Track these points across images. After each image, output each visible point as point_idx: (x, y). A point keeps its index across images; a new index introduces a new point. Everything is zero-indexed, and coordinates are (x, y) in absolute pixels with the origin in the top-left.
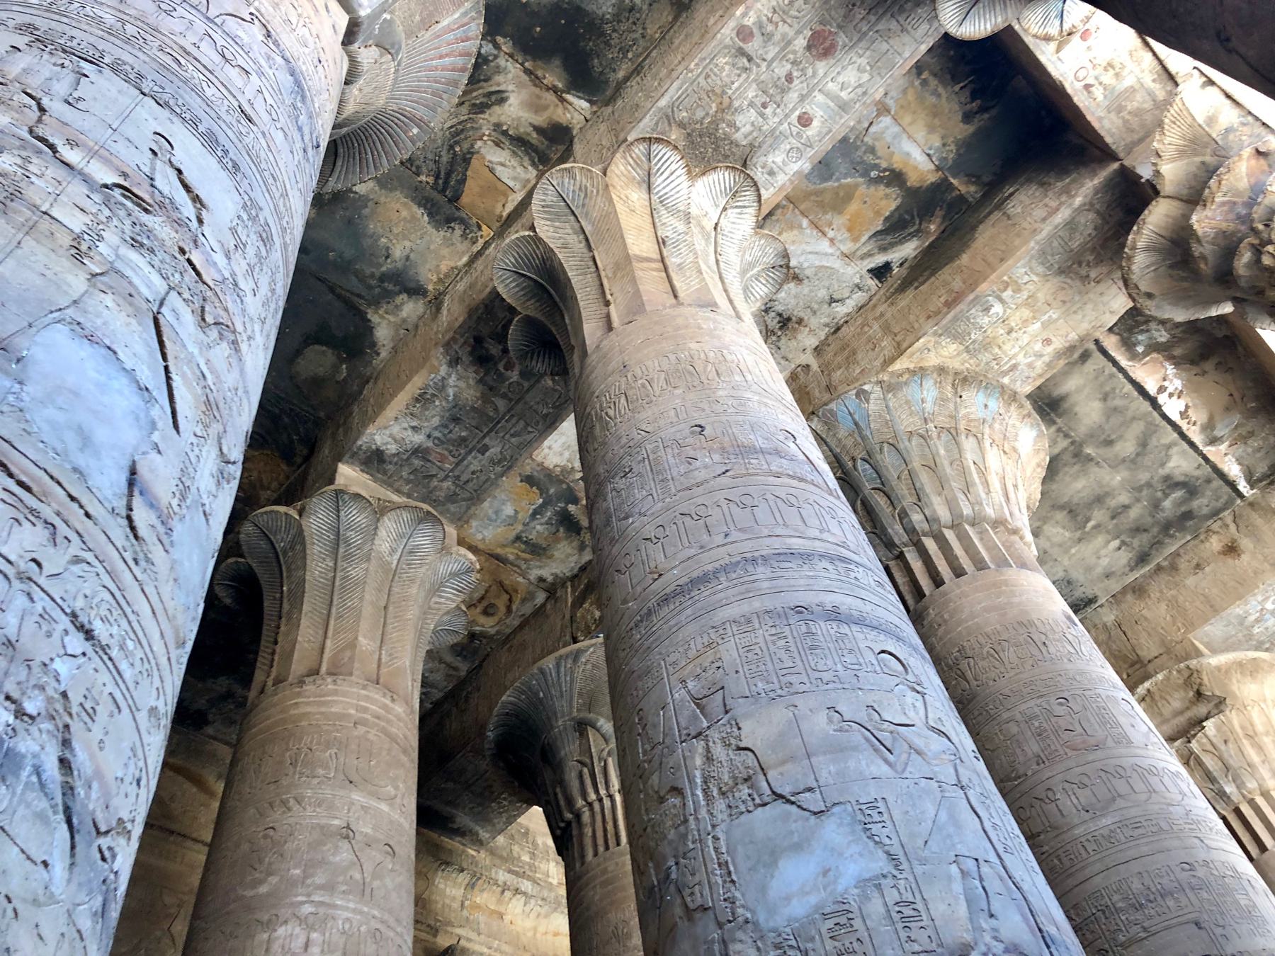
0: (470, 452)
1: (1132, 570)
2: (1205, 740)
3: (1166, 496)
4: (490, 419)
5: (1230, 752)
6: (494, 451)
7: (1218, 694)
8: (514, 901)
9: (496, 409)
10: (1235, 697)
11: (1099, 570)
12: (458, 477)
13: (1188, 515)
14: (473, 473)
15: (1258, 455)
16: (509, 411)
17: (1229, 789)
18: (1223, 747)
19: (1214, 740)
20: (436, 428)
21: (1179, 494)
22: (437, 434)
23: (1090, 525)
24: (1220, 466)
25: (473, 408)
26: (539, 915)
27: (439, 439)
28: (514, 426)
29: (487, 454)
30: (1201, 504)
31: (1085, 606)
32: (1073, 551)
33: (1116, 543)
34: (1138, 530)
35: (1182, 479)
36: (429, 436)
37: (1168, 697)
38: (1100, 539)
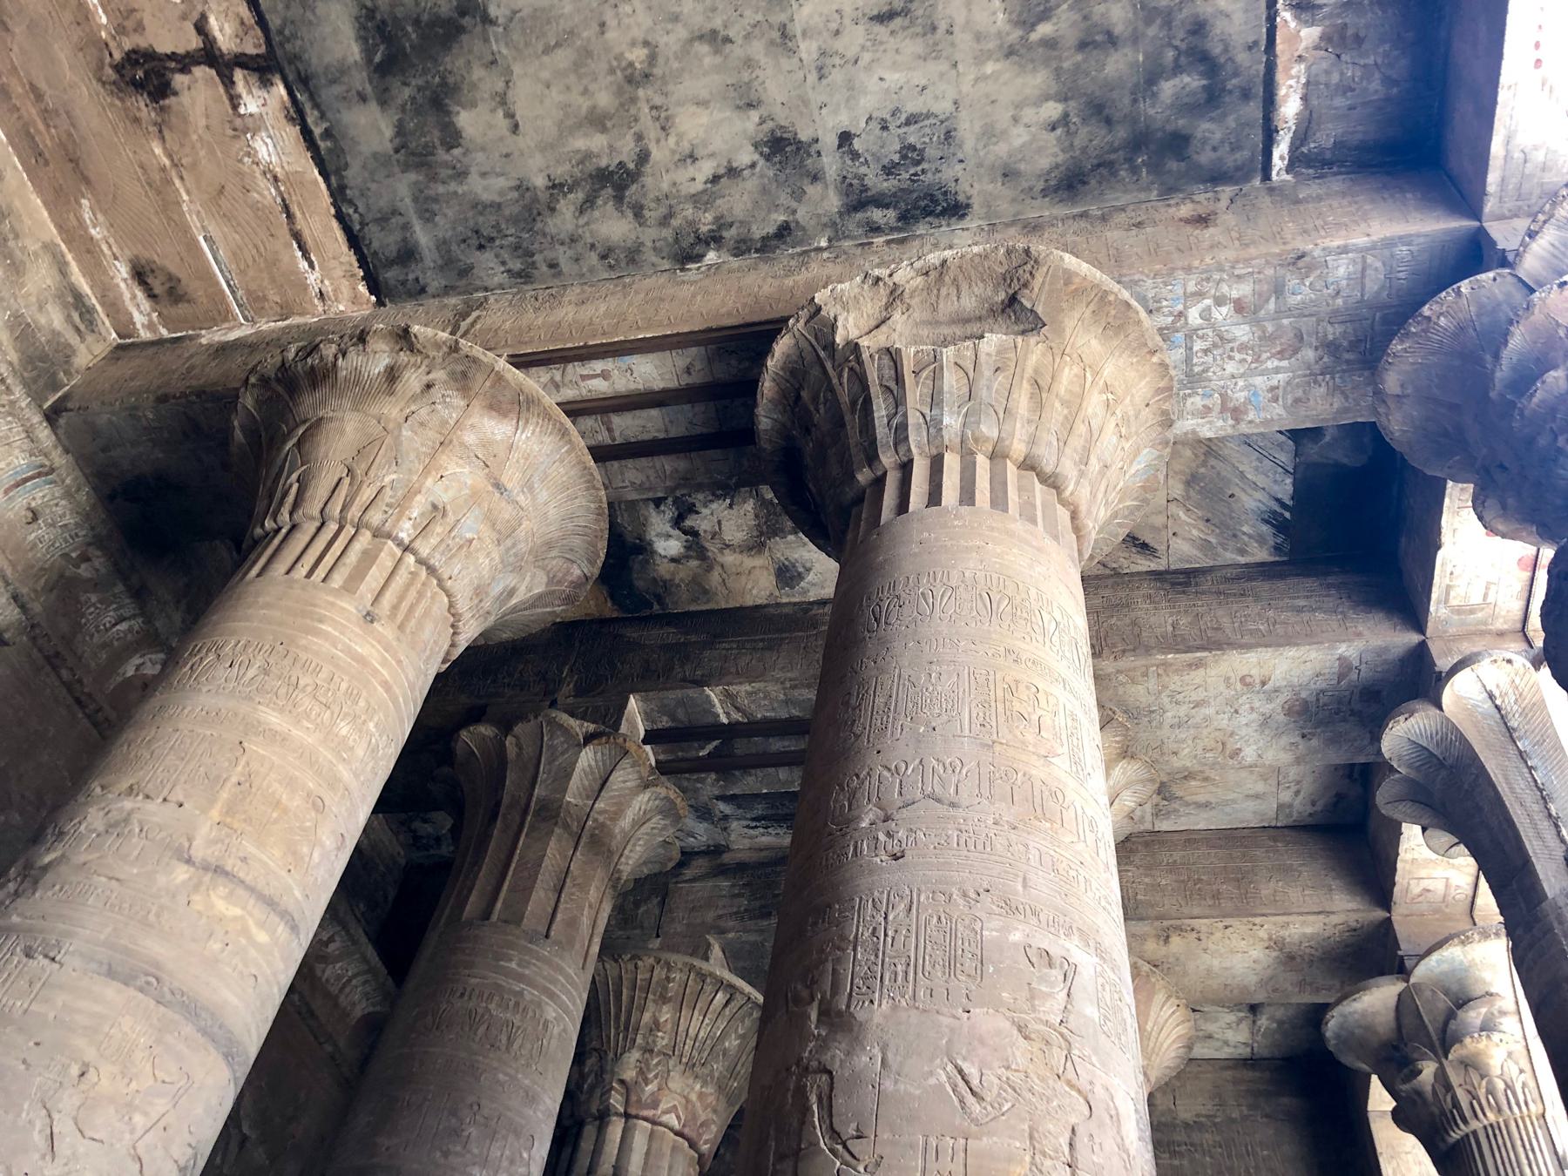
1: (1045, 193)
2: (969, 354)
3: (1177, 69)
5: (991, 387)
7: (1039, 310)
10: (1059, 331)
11: (1001, 149)
13: (1178, 143)
15: (1340, 102)
17: (951, 422)
18: (987, 373)
19: (982, 358)
21: (1192, 81)
23: (1044, 29)
24: (1280, 76)
30: (1208, 130)
31: (943, 213)
32: (990, 68)
33: (1053, 110)
34: (1098, 111)
35: (1217, 50)
37: (964, 287)
38: (1039, 80)
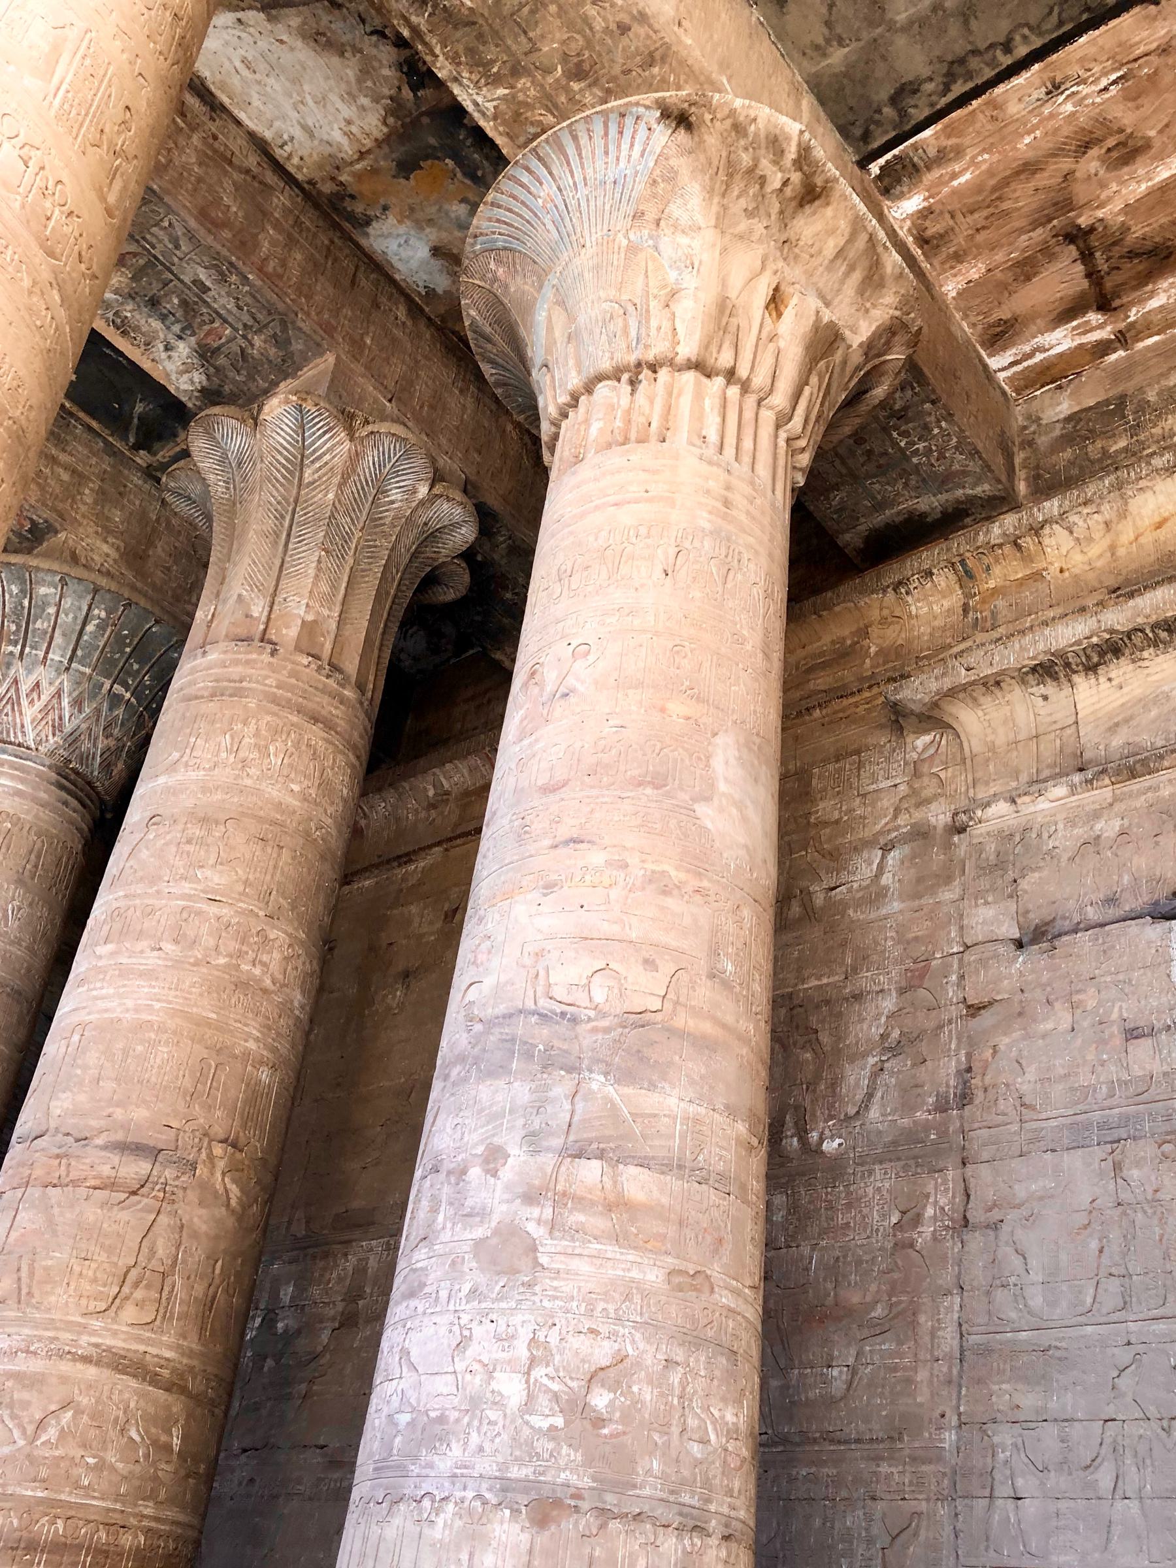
0: (205, 302)
4: (150, 264)
6: (203, 275)
8: (1046, 541)
9: (135, 255)
12: (245, 325)
14: (240, 308)
16: (137, 241)
20: (168, 328)
22: (176, 328)
25: (133, 279)
26: (1107, 524)
27: (183, 330)
28: (160, 241)
29: (208, 283)
36: (180, 338)
